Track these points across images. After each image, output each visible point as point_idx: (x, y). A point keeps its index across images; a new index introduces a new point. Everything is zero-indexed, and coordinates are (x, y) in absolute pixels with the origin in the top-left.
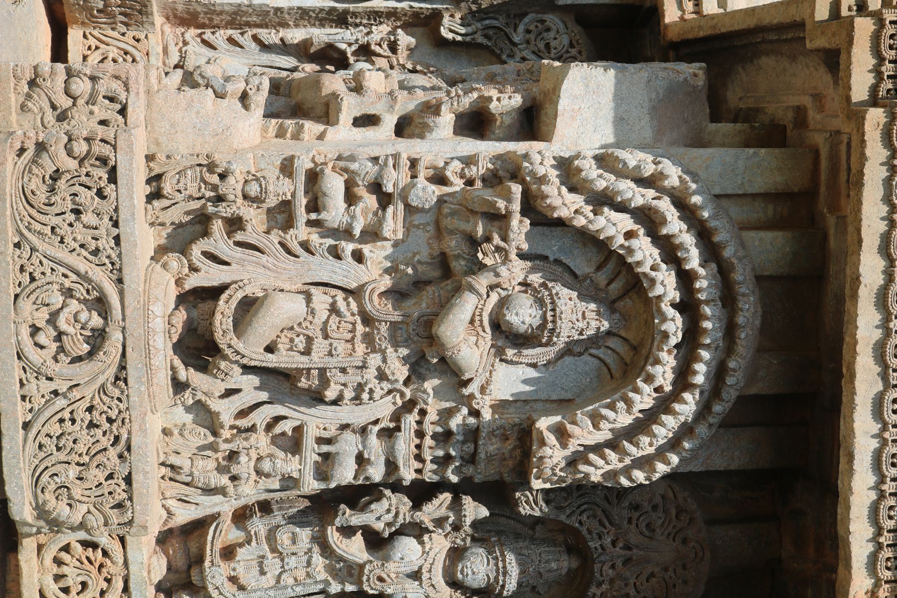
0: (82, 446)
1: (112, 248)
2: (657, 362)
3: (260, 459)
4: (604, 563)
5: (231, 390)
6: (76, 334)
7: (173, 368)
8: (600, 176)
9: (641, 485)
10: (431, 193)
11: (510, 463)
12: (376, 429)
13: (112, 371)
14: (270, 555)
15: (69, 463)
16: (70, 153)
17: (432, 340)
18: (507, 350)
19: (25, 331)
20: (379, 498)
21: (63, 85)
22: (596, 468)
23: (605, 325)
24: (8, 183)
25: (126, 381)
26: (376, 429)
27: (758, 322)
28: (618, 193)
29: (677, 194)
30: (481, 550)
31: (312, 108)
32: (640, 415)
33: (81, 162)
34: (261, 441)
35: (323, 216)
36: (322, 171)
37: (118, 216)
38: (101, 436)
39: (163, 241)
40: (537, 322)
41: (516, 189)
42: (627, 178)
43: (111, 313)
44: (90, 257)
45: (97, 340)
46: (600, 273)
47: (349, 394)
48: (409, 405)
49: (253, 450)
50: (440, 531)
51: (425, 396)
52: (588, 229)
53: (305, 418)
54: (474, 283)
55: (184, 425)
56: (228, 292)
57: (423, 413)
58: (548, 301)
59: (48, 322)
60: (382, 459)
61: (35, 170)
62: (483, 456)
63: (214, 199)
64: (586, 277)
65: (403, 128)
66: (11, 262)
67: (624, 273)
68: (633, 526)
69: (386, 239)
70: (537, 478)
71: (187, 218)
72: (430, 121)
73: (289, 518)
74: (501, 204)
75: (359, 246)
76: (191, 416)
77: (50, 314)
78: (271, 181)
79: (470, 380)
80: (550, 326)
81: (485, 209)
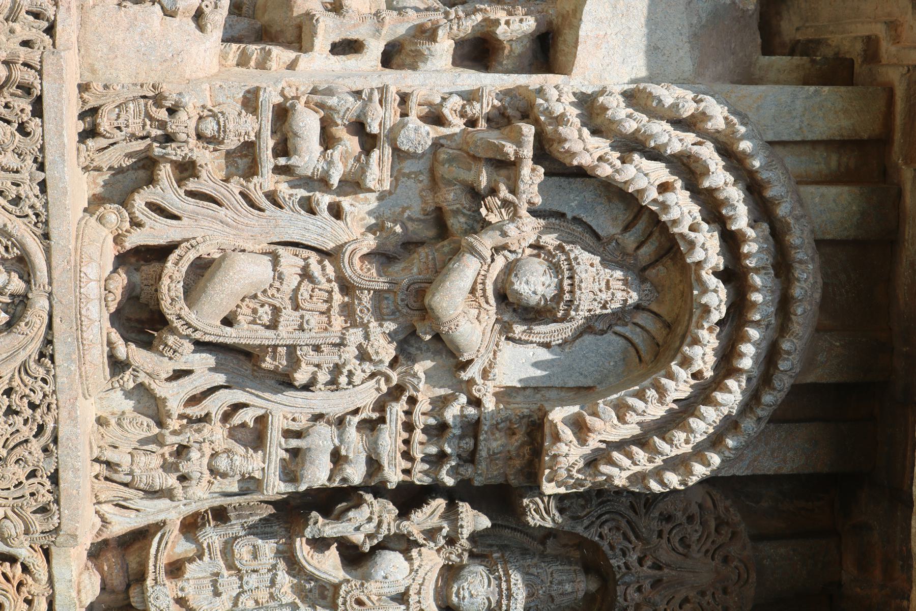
1: (37, 197)
2: (696, 341)
3: (214, 455)
4: (628, 585)
5: (180, 372)
7: (110, 344)
8: (629, 116)
9: (675, 491)
10: (424, 134)
11: (518, 463)
12: (356, 420)
13: (36, 345)
14: (225, 573)
17: (425, 312)
18: (514, 326)
20: (358, 503)
22: (621, 469)
23: (634, 297)
26: (356, 420)
27: (817, 296)
28: (651, 136)
29: (722, 138)
30: (481, 569)
31: (282, 31)
32: (675, 406)
34: (217, 433)
36: (293, 106)
37: (43, 157)
39: (99, 190)
40: (551, 292)
41: (529, 131)
42: (662, 118)
43: (35, 275)
44: (10, 207)
46: (627, 235)
47: (323, 377)
48: (396, 392)
49: (207, 444)
50: (432, 544)
51: (415, 381)
52: (615, 180)
53: (270, 406)
54: (476, 243)
55: (123, 413)
56: (177, 252)
57: (412, 401)
58: (565, 267)
60: (363, 457)
62: (484, 453)
63: (162, 139)
64: (611, 238)
65: (391, 57)
67: (656, 234)
68: (664, 541)
69: (370, 190)
70: (550, 481)
71: (129, 162)
72: (424, 47)
73: (250, 527)
74: (510, 149)
75: (338, 199)
78: (231, 118)
79: (470, 362)
80: (567, 297)
81: (490, 155)
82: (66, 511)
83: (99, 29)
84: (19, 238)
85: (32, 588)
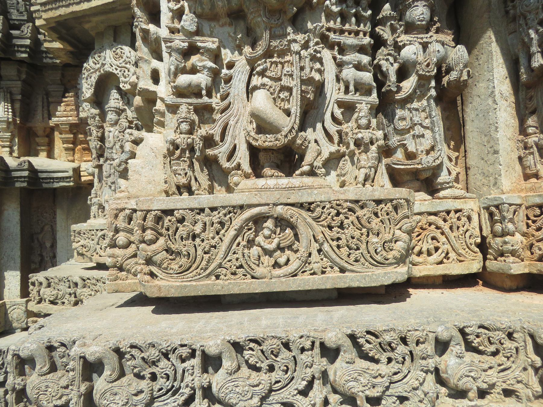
0: (356, 233)
1: (219, 213)
3: (359, 127)
6: (279, 238)
7: (302, 174)
10: (187, 17)
12: (339, 57)
13: (304, 213)
14: (412, 133)
15: (368, 242)
16: (153, 242)
19: (278, 272)
21: (121, 250)
24: (174, 284)
25: (310, 204)
33: (161, 235)
34: (348, 127)
35: (203, 86)
37: (196, 209)
38: (349, 220)
39: (223, 189)
43: (263, 213)
44: (226, 228)
45: (282, 223)
47: (318, 66)
51: (318, 28)
53: (332, 101)
56: (251, 141)
57: (329, 29)
59: (271, 256)
61: (165, 265)
66: (229, 281)
73: (390, 122)
76: (332, 172)
77: (266, 255)
82: (397, 195)
83: (140, 189)
84: (242, 222)
85: (424, 223)
